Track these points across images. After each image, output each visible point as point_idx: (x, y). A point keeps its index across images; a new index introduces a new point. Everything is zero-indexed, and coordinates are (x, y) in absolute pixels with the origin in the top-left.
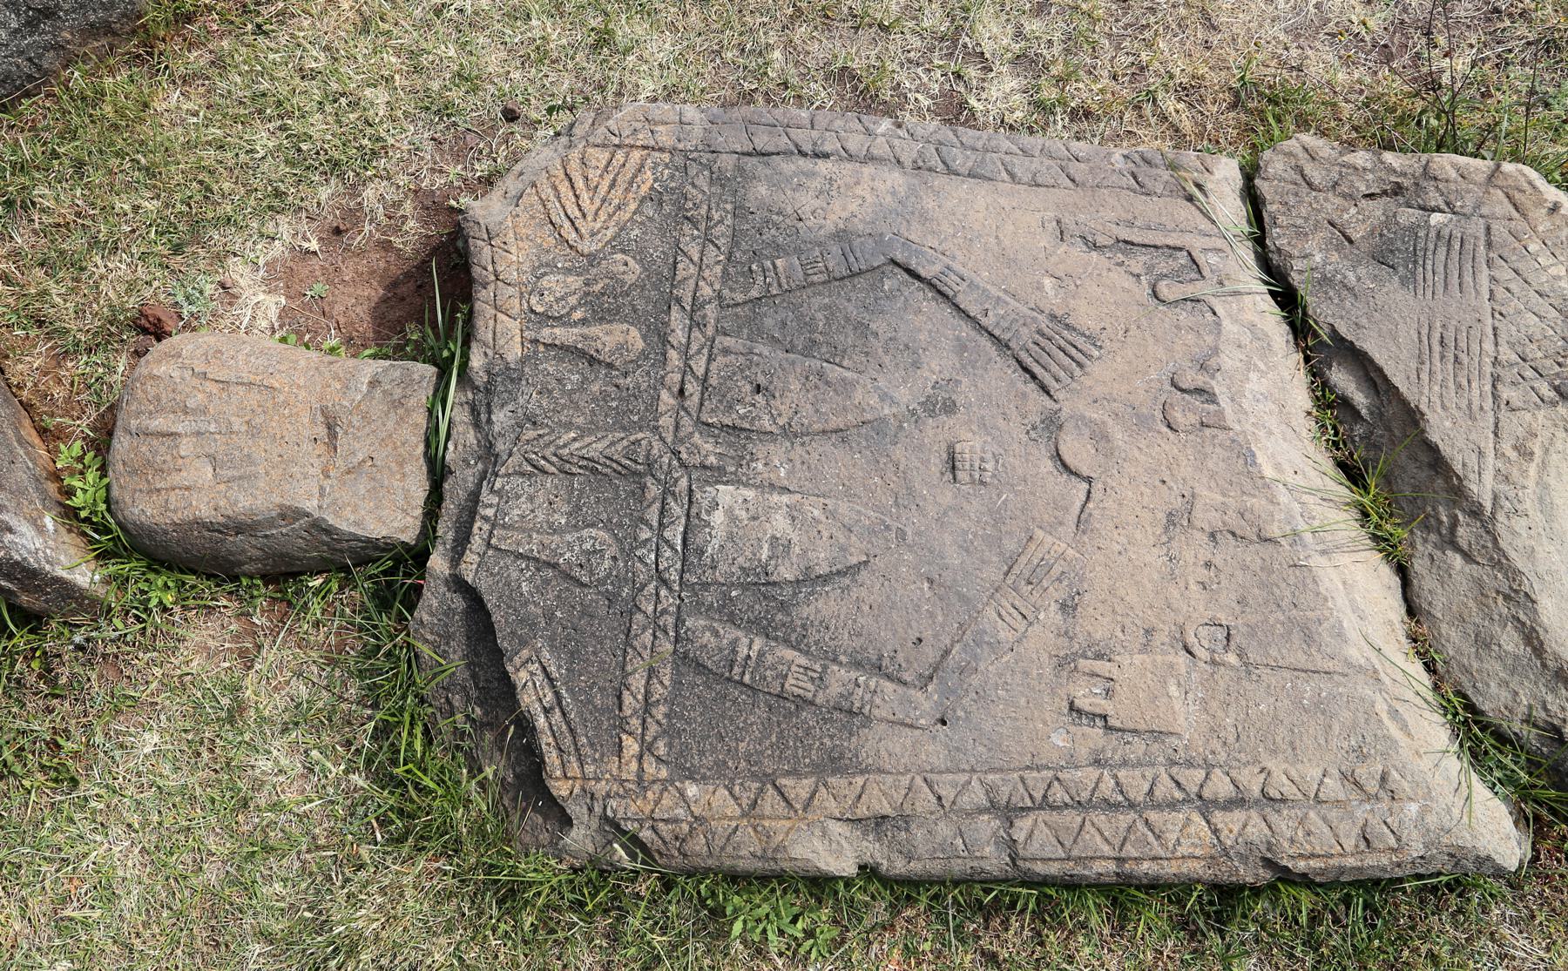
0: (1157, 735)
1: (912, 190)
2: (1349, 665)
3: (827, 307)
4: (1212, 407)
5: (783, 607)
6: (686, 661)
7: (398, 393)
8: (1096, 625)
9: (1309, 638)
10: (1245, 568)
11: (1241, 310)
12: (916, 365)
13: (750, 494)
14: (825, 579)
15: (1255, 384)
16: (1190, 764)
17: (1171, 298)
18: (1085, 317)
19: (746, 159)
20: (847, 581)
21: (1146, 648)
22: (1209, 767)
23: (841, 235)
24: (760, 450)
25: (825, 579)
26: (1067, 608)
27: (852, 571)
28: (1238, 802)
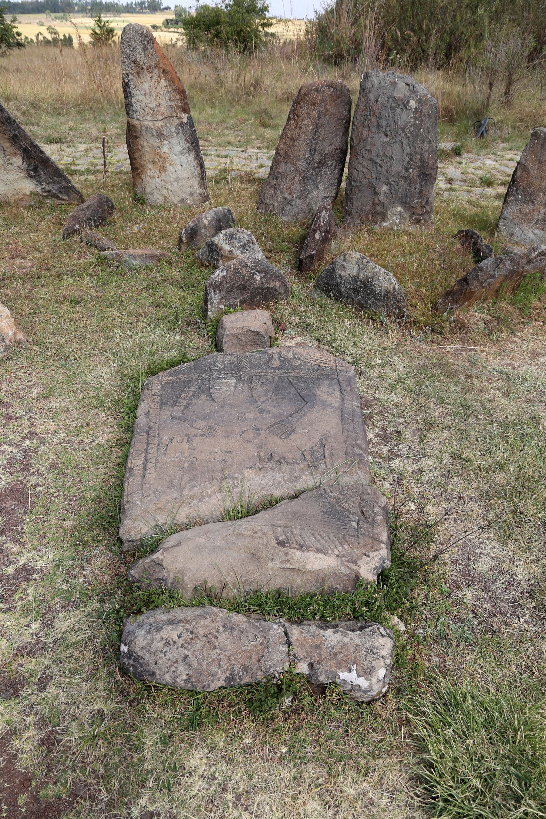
0: (165, 454)
1: (334, 407)
2: (183, 488)
3: (290, 393)
4: (266, 460)
5: (203, 392)
6: (190, 382)
7: (259, 343)
8: (197, 440)
9: (191, 480)
10: (214, 467)
11: (306, 475)
12: (274, 407)
13: (234, 384)
14: (211, 397)
15: (279, 476)
16: (156, 460)
17: (305, 453)
18: (293, 436)
19: (336, 381)
20: (210, 399)
21: (189, 449)
22: (155, 463)
23: (315, 395)
24: (246, 386)
25: (211, 397)
26: (202, 435)
27: (213, 400)
28: (145, 469)
